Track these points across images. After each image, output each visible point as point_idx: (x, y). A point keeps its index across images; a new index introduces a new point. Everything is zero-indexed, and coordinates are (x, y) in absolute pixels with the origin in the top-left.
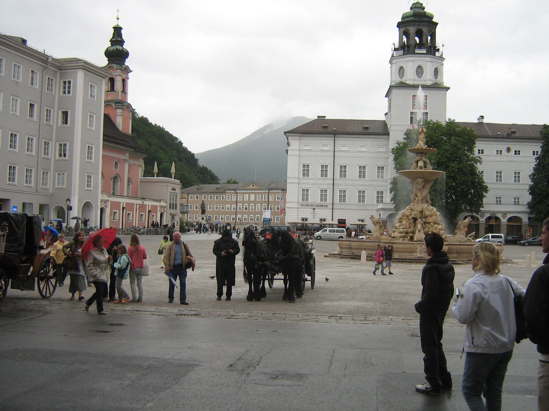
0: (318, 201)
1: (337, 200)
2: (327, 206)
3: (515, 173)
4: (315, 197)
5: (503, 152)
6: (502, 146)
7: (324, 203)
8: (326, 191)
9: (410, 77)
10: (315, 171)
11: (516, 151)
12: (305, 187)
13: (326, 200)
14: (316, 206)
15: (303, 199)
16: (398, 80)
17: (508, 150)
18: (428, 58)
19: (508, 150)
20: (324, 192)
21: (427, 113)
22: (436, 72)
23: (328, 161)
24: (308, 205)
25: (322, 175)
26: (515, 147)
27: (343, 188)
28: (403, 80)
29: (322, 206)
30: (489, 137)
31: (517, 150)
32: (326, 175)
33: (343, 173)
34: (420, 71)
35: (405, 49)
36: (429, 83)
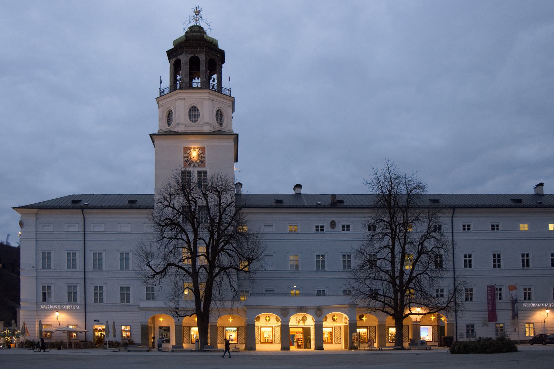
3: (344, 256)
5: (325, 229)
6: (324, 220)
11: (343, 226)
16: (166, 128)
17: (333, 225)
18: (205, 94)
19: (333, 225)
22: (219, 115)
25: (69, 267)
26: (341, 219)
30: (304, 207)
31: (346, 224)
32: (74, 266)
34: (194, 113)
36: (207, 129)
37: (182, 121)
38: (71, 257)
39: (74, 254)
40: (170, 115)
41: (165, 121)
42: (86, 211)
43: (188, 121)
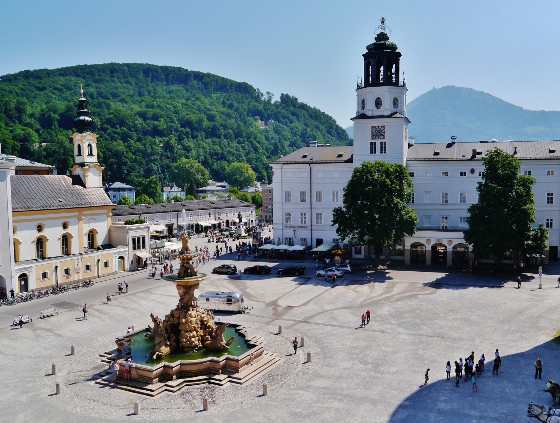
0: (299, 224)
1: (314, 222)
2: (306, 227)
4: (296, 220)
7: (303, 225)
8: (305, 214)
9: (371, 109)
10: (296, 196)
12: (288, 211)
13: (305, 222)
14: (298, 227)
15: (287, 222)
16: (362, 112)
20: (303, 215)
21: (385, 143)
23: (307, 188)
24: (291, 227)
27: (319, 212)
28: (364, 112)
29: (303, 227)
32: (305, 201)
33: (319, 199)
35: (371, 80)
36: (387, 113)
37: (371, 108)
38: (303, 193)
39: (305, 193)
40: (363, 104)
41: (360, 106)
42: (311, 165)
43: (375, 108)
